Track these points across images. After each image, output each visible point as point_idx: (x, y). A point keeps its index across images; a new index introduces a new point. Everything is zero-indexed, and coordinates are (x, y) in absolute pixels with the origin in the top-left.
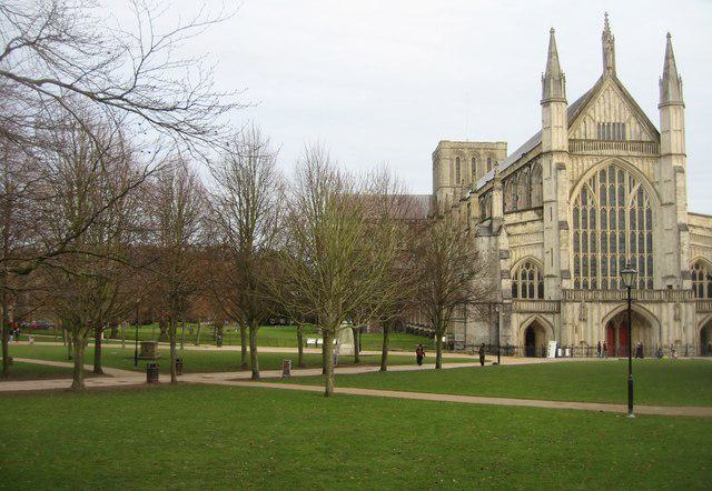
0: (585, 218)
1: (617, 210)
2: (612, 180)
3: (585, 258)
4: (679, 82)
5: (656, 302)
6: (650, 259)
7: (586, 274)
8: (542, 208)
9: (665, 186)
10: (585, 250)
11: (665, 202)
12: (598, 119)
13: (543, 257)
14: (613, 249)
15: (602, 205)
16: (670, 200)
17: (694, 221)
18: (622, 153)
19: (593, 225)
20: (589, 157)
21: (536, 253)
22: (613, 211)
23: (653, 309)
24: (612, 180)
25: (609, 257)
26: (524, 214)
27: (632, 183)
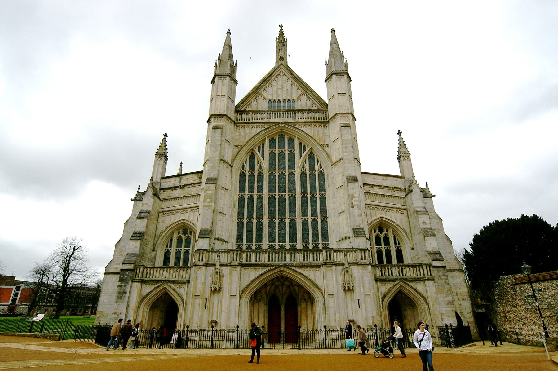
0: (251, 182)
1: (287, 174)
2: (282, 146)
3: (250, 223)
5: (318, 266)
6: (324, 222)
7: (249, 240)
10: (250, 214)
14: (282, 213)
15: (270, 169)
17: (370, 180)
18: (290, 120)
19: (260, 189)
20: (255, 125)
22: (282, 175)
24: (282, 146)
25: (277, 221)
27: (302, 147)
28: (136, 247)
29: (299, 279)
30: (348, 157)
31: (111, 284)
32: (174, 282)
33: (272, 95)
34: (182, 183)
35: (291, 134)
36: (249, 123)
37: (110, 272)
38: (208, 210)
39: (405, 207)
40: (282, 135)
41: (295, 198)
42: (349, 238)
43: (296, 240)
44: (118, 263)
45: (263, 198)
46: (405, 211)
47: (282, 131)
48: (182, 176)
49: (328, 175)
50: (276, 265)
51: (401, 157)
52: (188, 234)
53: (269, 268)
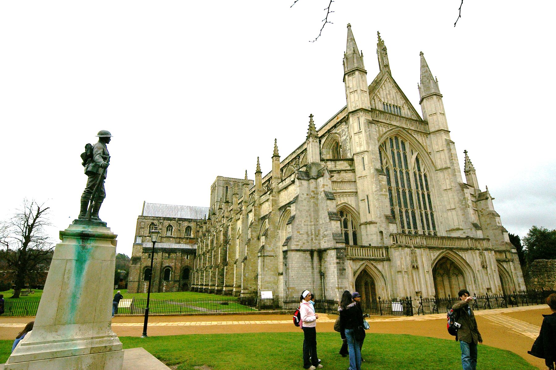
2: (398, 147)
4: (436, 82)
5: (467, 250)
8: (352, 160)
9: (438, 155)
11: (438, 169)
12: (383, 100)
13: (358, 205)
16: (444, 166)
21: (351, 201)
23: (467, 256)
24: (398, 147)
26: (338, 163)
28: (338, 227)
29: (456, 260)
30: (457, 168)
31: (296, 260)
32: (374, 260)
33: (384, 98)
34: (337, 168)
35: (403, 138)
36: (378, 121)
37: (292, 248)
38: (386, 199)
39: (476, 209)
40: (396, 137)
41: (412, 193)
42: (463, 229)
43: (417, 227)
44: (297, 240)
45: (391, 190)
46: (477, 212)
47: (397, 134)
48: (336, 162)
49: (431, 178)
50: (446, 248)
51: (471, 171)
52: (345, 217)
53: (442, 251)
